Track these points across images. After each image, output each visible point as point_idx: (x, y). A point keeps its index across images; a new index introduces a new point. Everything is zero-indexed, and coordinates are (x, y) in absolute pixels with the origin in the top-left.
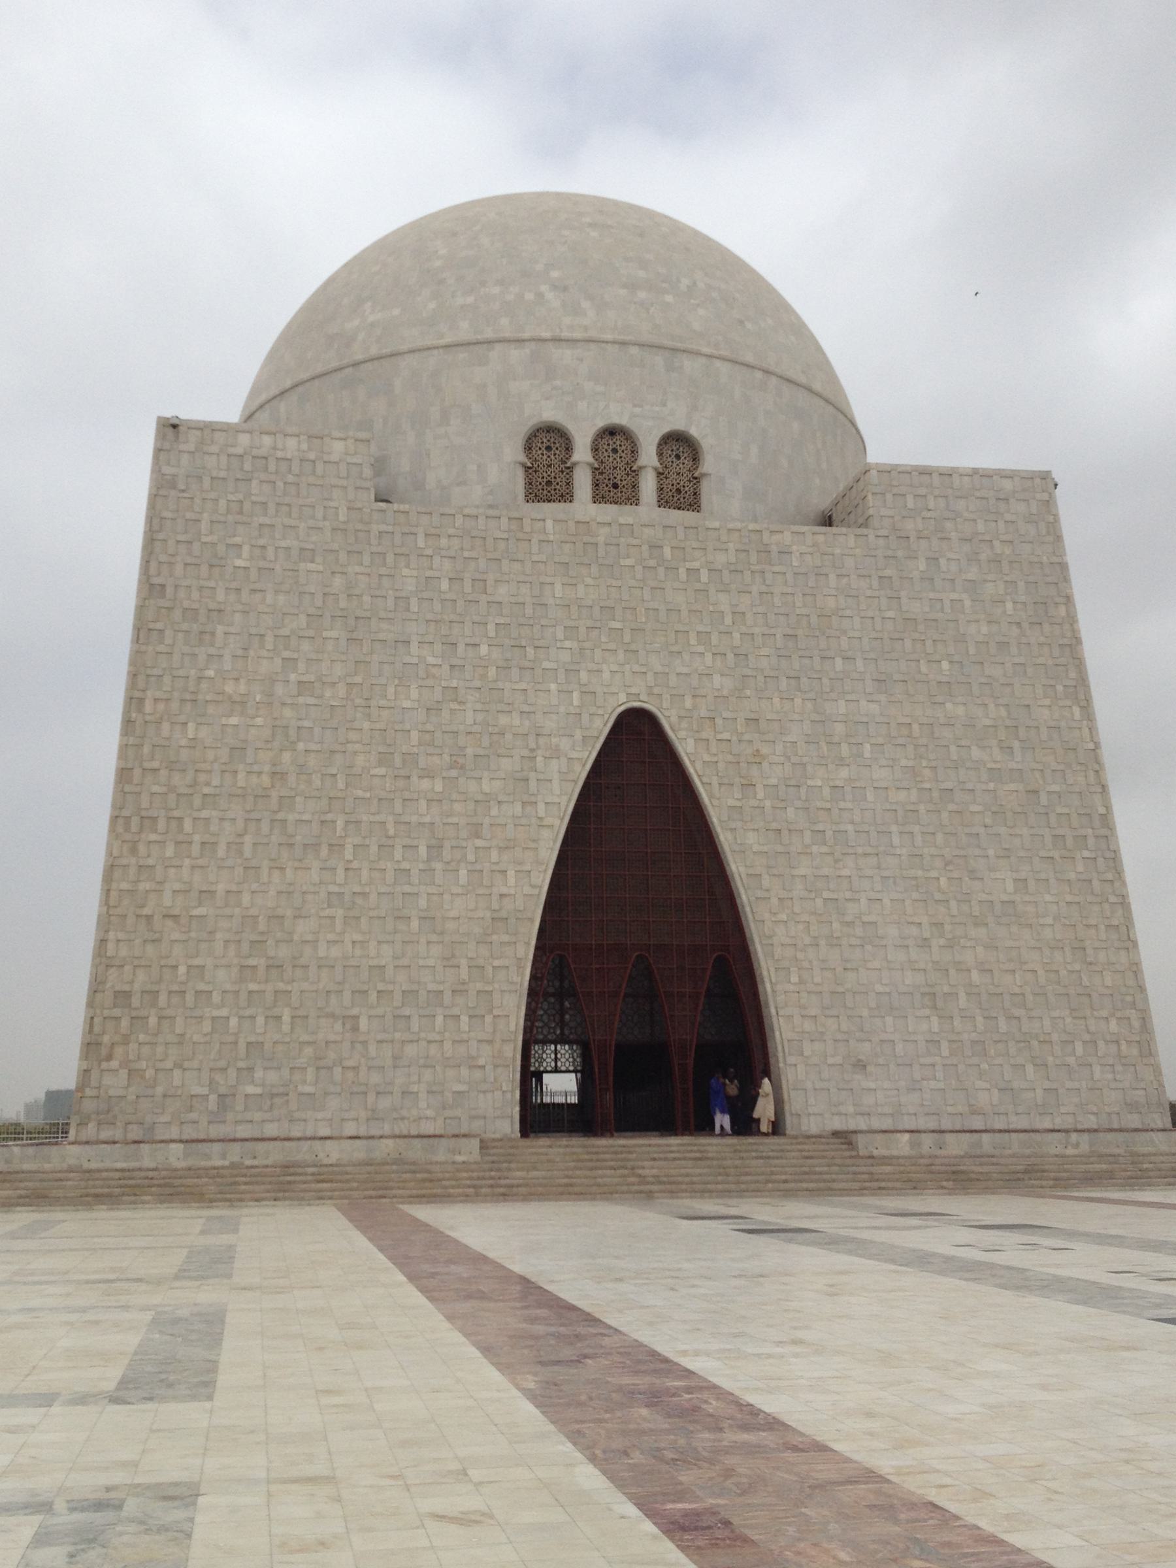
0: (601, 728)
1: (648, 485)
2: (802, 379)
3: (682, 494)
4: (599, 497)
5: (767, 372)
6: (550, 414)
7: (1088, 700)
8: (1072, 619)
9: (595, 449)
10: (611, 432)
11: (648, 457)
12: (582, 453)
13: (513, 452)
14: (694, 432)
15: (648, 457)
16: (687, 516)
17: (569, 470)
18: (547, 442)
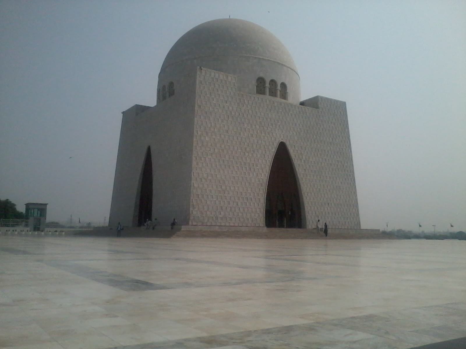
0: (276, 145)
3: (284, 96)
6: (262, 75)
13: (254, 82)
15: (279, 87)
16: (283, 100)
17: (265, 87)
18: (261, 81)
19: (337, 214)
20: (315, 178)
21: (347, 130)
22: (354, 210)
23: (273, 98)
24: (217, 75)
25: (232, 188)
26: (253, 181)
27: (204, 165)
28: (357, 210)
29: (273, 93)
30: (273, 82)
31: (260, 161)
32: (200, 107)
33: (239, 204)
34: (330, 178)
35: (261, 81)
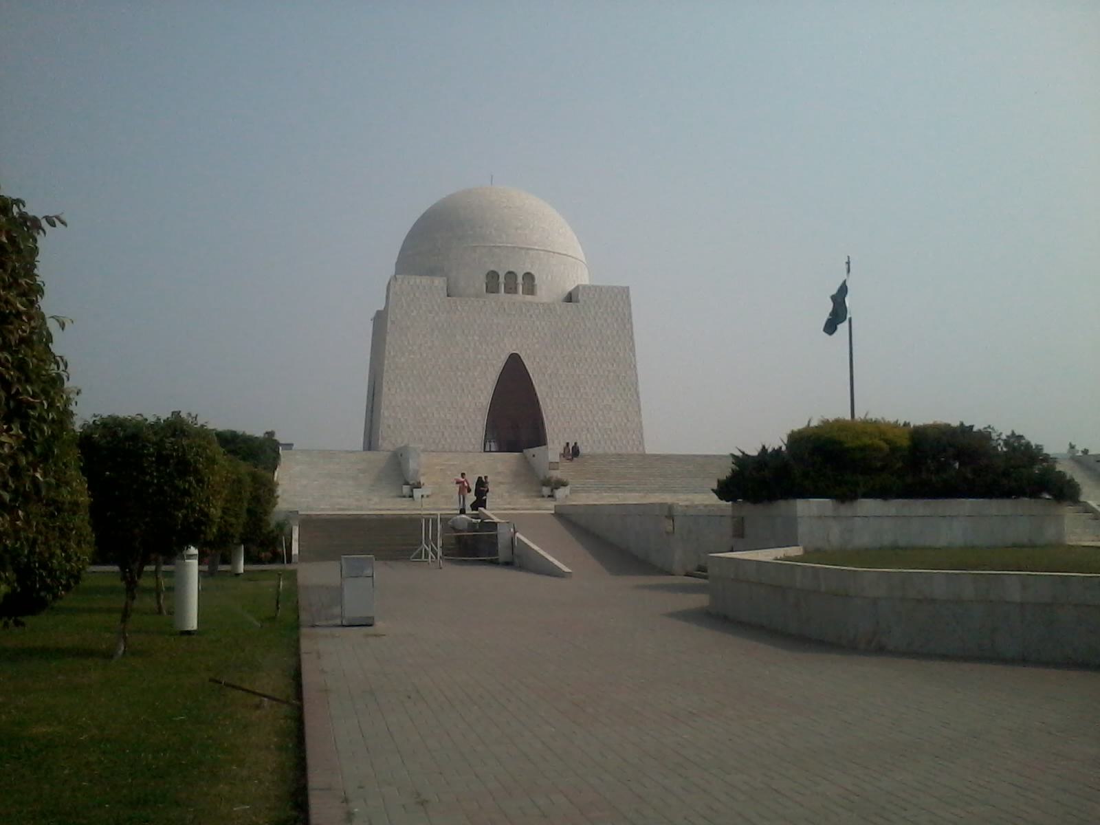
0: (504, 358)
1: (520, 288)
2: (565, 253)
3: (530, 288)
4: (506, 292)
5: (554, 253)
6: (492, 268)
7: (634, 351)
8: (632, 328)
9: (505, 279)
10: (510, 273)
11: (520, 280)
12: (502, 279)
14: (533, 272)
15: (520, 280)
18: (493, 276)
19: (602, 442)
20: (567, 396)
21: (628, 326)
22: (634, 437)
23: (514, 297)
24: (418, 281)
25: (436, 415)
26: (467, 405)
27: (398, 390)
28: (640, 436)
29: (510, 289)
30: (511, 275)
31: (478, 380)
32: (393, 322)
33: (446, 434)
34: (593, 395)
35: (493, 276)
